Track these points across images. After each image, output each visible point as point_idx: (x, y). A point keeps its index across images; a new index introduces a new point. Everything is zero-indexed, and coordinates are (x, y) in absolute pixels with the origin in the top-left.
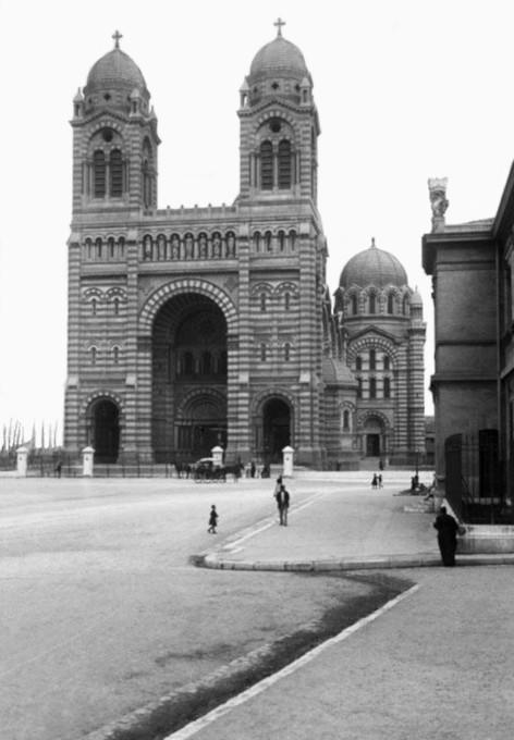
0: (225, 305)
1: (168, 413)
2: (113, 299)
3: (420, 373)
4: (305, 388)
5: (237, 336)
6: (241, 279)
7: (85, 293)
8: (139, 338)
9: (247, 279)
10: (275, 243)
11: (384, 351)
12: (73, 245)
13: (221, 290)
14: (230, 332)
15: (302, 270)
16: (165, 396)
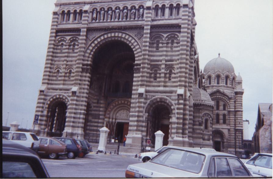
0: (134, 47)
1: (101, 113)
2: (72, 43)
3: (240, 112)
4: (180, 97)
5: (139, 65)
6: (145, 31)
7: (58, 40)
8: (83, 65)
9: (149, 31)
10: (167, 11)
11: (224, 102)
12: (55, 13)
13: (133, 38)
14: (136, 62)
15: (182, 26)
16: (101, 103)
